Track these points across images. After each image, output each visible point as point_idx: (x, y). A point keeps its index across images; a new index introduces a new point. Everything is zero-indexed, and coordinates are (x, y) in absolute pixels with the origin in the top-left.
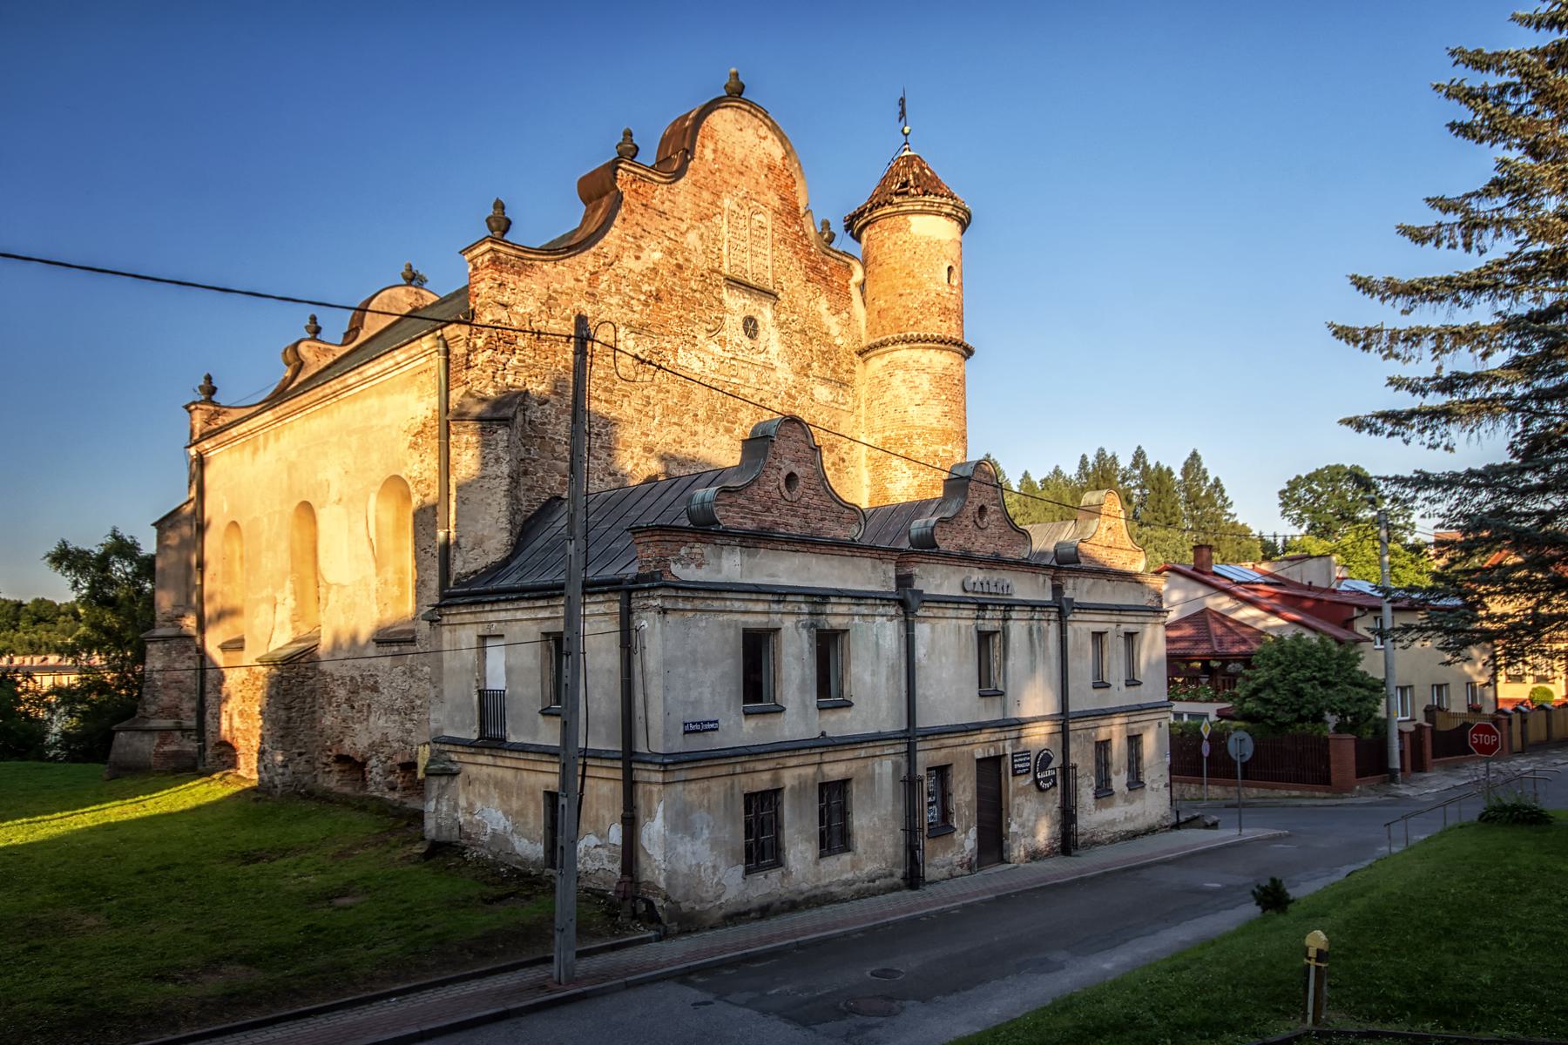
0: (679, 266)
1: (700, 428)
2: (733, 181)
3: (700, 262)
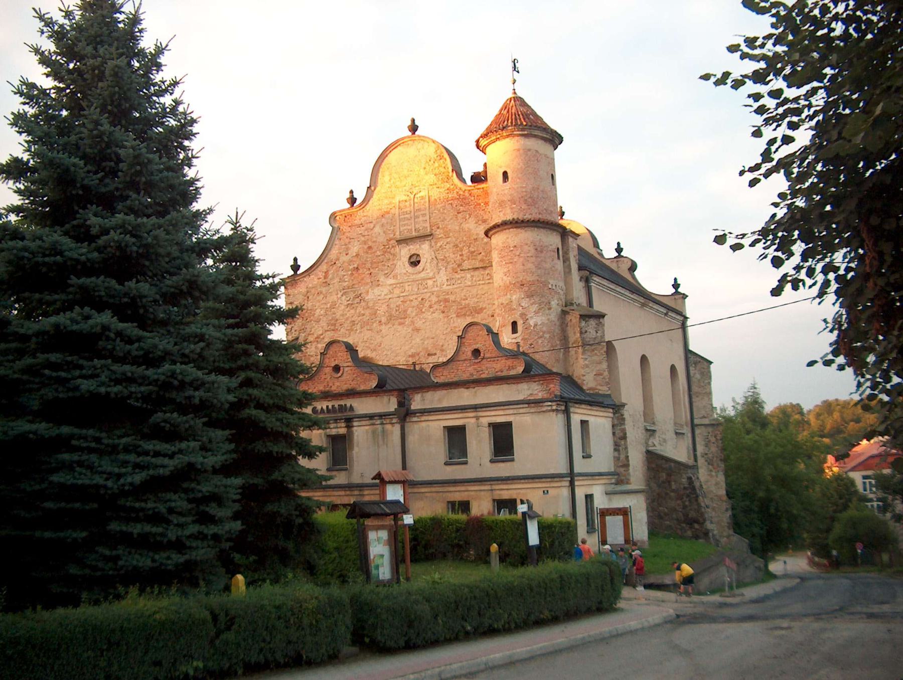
0: (370, 248)
1: (383, 327)
2: (404, 183)
3: (382, 239)
